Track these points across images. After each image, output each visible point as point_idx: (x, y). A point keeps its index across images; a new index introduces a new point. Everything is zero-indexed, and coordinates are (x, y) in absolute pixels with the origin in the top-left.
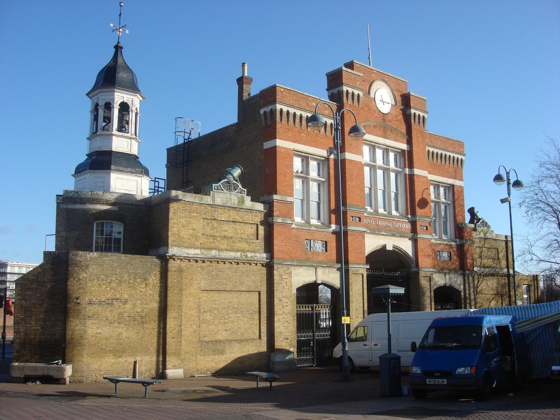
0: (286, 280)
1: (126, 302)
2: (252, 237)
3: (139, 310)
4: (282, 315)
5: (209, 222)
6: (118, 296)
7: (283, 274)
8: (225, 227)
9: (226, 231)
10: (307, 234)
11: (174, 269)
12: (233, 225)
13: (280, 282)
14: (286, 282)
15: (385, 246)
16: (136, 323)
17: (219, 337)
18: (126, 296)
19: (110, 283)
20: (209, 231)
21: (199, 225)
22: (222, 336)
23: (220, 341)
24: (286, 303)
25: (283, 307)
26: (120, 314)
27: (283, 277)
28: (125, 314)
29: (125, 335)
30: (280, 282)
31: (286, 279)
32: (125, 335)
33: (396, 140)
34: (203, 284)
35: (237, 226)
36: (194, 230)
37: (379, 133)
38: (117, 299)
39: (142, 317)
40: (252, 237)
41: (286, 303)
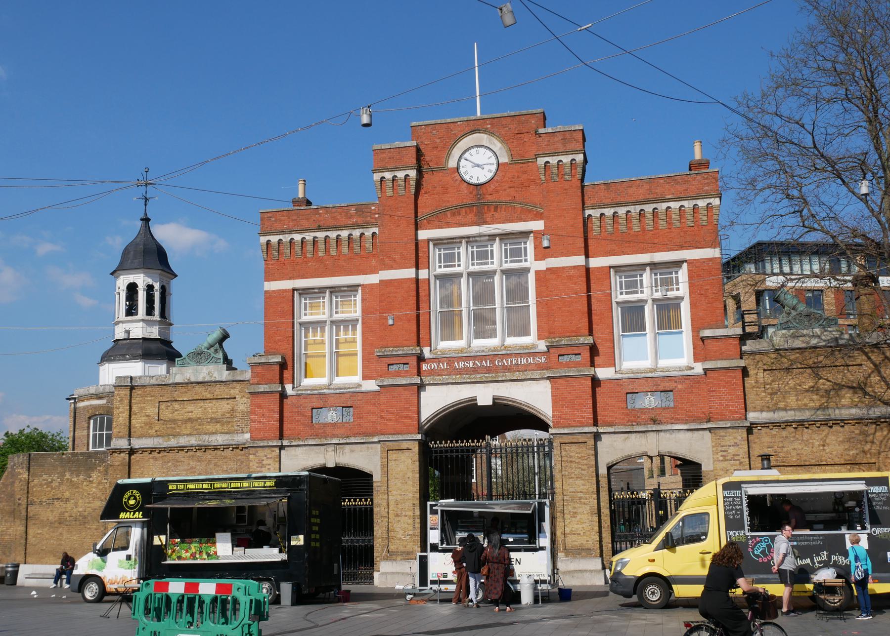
0: (268, 467)
1: (67, 500)
2: (228, 415)
3: (81, 510)
5: (169, 404)
6: (59, 495)
7: (265, 458)
8: (190, 407)
9: (192, 412)
10: (315, 400)
11: (117, 464)
12: (201, 403)
16: (78, 523)
18: (67, 494)
19: (51, 482)
26: (62, 513)
27: (264, 462)
28: (66, 514)
35: (207, 404)
36: (147, 416)
38: (58, 499)
39: (85, 517)
40: (228, 415)
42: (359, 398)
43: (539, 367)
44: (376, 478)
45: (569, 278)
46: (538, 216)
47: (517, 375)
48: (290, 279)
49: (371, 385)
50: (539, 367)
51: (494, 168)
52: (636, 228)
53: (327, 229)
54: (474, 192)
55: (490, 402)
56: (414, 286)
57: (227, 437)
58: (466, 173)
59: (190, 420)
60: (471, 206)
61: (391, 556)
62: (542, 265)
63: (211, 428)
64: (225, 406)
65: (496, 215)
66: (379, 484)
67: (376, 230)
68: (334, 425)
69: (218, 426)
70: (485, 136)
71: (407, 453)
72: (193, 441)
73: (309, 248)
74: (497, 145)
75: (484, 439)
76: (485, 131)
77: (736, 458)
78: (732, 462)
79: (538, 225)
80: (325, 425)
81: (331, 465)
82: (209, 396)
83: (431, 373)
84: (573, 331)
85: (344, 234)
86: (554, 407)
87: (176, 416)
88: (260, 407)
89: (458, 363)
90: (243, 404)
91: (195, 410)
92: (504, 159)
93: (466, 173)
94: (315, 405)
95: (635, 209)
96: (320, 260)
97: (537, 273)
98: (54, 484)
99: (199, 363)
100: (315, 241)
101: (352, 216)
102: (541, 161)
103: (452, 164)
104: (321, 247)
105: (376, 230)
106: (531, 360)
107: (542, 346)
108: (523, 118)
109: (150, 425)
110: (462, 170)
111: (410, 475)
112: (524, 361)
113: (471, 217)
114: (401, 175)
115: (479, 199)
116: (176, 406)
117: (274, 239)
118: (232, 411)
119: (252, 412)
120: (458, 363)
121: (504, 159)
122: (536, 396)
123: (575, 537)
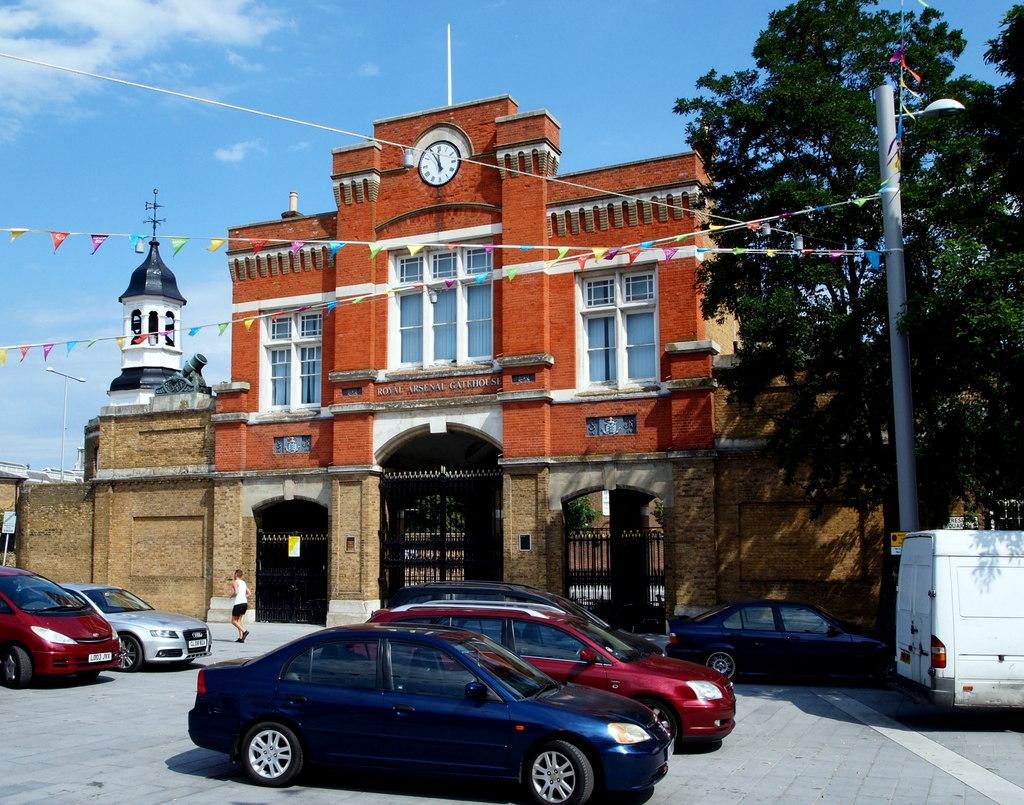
4: (223, 546)
8: (166, 437)
15: (427, 426)
17: (154, 573)
20: (146, 446)
21: (134, 441)
22: (156, 571)
23: (153, 578)
29: (60, 566)
32: (60, 566)
33: (467, 225)
34: (136, 510)
35: (181, 435)
37: (427, 226)
45: (526, 287)
48: (258, 299)
54: (435, 195)
55: (442, 429)
58: (428, 174)
59: (165, 451)
60: (430, 211)
61: (342, 596)
63: (180, 459)
72: (170, 471)
74: (458, 142)
75: (439, 470)
81: (289, 497)
84: (528, 348)
86: (505, 434)
87: (153, 446)
91: (170, 441)
93: (428, 174)
98: (51, 516)
99: (175, 392)
109: (131, 456)
110: (424, 172)
113: (431, 221)
115: (439, 202)
116: (154, 437)
121: (465, 155)
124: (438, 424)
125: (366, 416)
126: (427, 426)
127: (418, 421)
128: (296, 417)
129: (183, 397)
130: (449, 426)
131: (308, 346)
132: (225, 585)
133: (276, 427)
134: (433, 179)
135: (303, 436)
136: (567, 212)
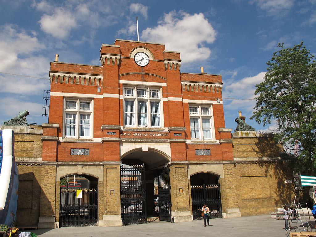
2: (29, 149)
13: (46, 174)
14: (51, 174)
15: (141, 148)
24: (51, 187)
25: (48, 190)
27: (48, 171)
30: (46, 174)
31: (51, 172)
41: (51, 187)
42: (92, 145)
43: (165, 137)
44: (100, 179)
45: (177, 105)
46: (164, 82)
47: (158, 140)
49: (99, 140)
50: (165, 137)
51: (148, 61)
52: (197, 90)
53: (81, 74)
54: (141, 69)
56: (118, 101)
57: (28, 159)
60: (139, 74)
61: (108, 213)
62: (166, 100)
64: (28, 145)
65: (149, 78)
66: (101, 182)
67: (102, 78)
68: (81, 156)
69: (25, 154)
70: (145, 49)
71: (115, 169)
73: (72, 80)
74: (148, 53)
76: (144, 48)
77: (232, 174)
78: (230, 175)
79: (164, 85)
80: (77, 156)
82: (20, 140)
83: (124, 137)
85: (88, 77)
88: (47, 146)
89: (135, 134)
90: (38, 144)
92: (151, 59)
94: (73, 147)
95: (197, 84)
96: (76, 86)
97: (164, 102)
99: (16, 124)
100: (75, 77)
101: (91, 70)
102: (166, 62)
103: (132, 57)
104: (77, 81)
105: (102, 78)
106: (163, 135)
107: (167, 130)
108: (158, 46)
111: (116, 178)
112: (160, 135)
113: (140, 78)
114: (114, 57)
115: (142, 71)
117: (57, 74)
118: (32, 148)
119: (42, 148)
120: (135, 134)
121: (151, 59)
122: (165, 149)
123: (181, 203)
124: (145, 148)
125: (120, 143)
126: (141, 148)
127: (138, 146)
128: (82, 141)
129: (21, 127)
130: (149, 149)
131: (83, 114)
132: (47, 211)
133: (72, 144)
134: (146, 62)
135: (85, 149)
136: (194, 85)
